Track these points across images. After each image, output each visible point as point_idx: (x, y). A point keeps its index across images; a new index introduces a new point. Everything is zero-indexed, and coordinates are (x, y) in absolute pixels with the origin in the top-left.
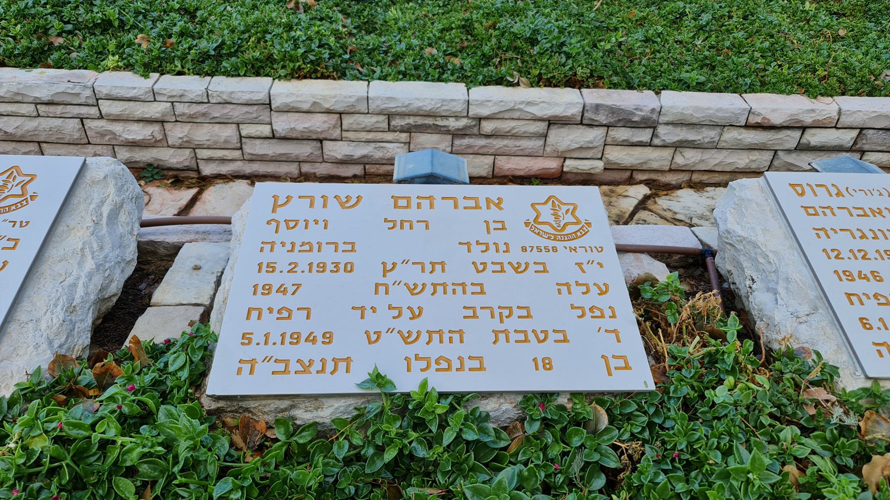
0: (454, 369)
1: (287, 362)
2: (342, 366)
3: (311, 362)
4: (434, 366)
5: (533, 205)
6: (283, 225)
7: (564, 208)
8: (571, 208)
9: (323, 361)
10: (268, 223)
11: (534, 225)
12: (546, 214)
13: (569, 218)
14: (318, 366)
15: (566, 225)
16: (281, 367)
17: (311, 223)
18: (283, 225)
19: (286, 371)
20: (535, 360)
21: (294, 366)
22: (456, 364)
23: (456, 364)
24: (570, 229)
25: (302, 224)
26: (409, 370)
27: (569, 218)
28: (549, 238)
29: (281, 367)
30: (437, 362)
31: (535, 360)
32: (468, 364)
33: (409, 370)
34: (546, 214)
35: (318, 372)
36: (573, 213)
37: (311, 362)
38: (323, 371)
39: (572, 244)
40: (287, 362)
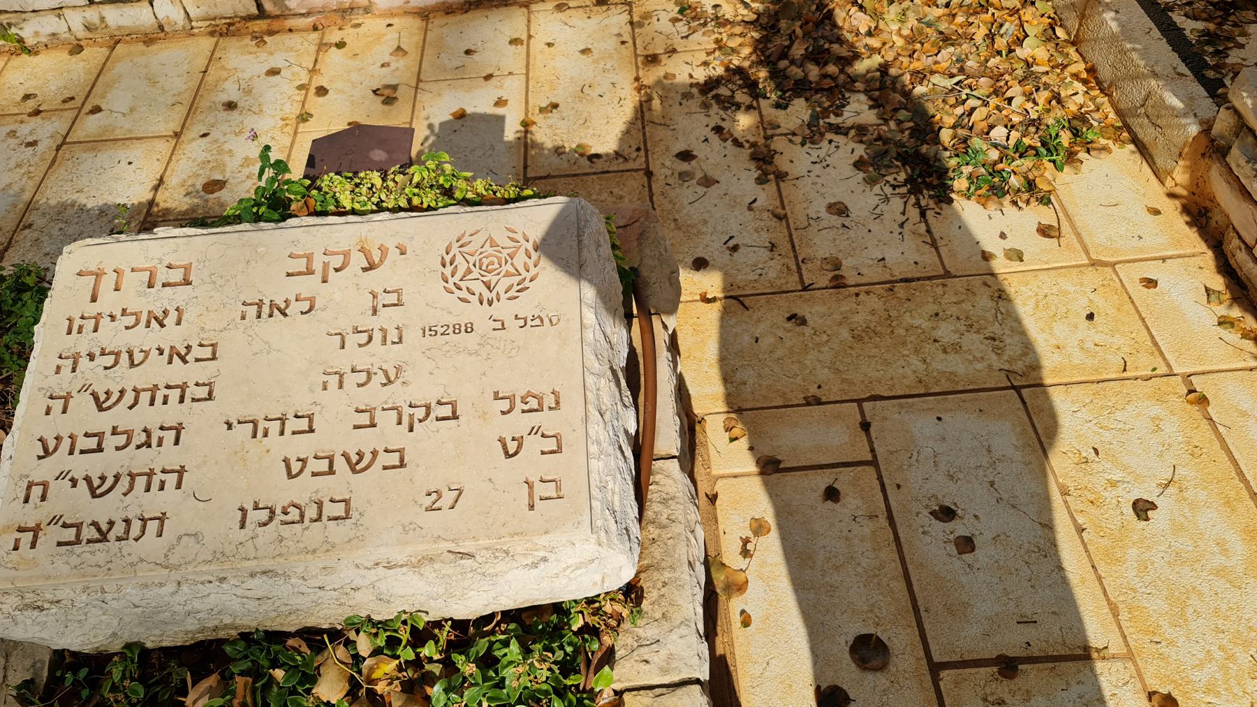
0: (306, 520)
1: (78, 526)
2: (153, 526)
3: (111, 523)
4: (280, 517)
9: (127, 521)
14: (119, 529)
16: (70, 534)
19: (78, 541)
21: (89, 533)
22: (311, 512)
23: (311, 512)
29: (70, 534)
35: (119, 539)
37: (111, 523)
40: (78, 526)
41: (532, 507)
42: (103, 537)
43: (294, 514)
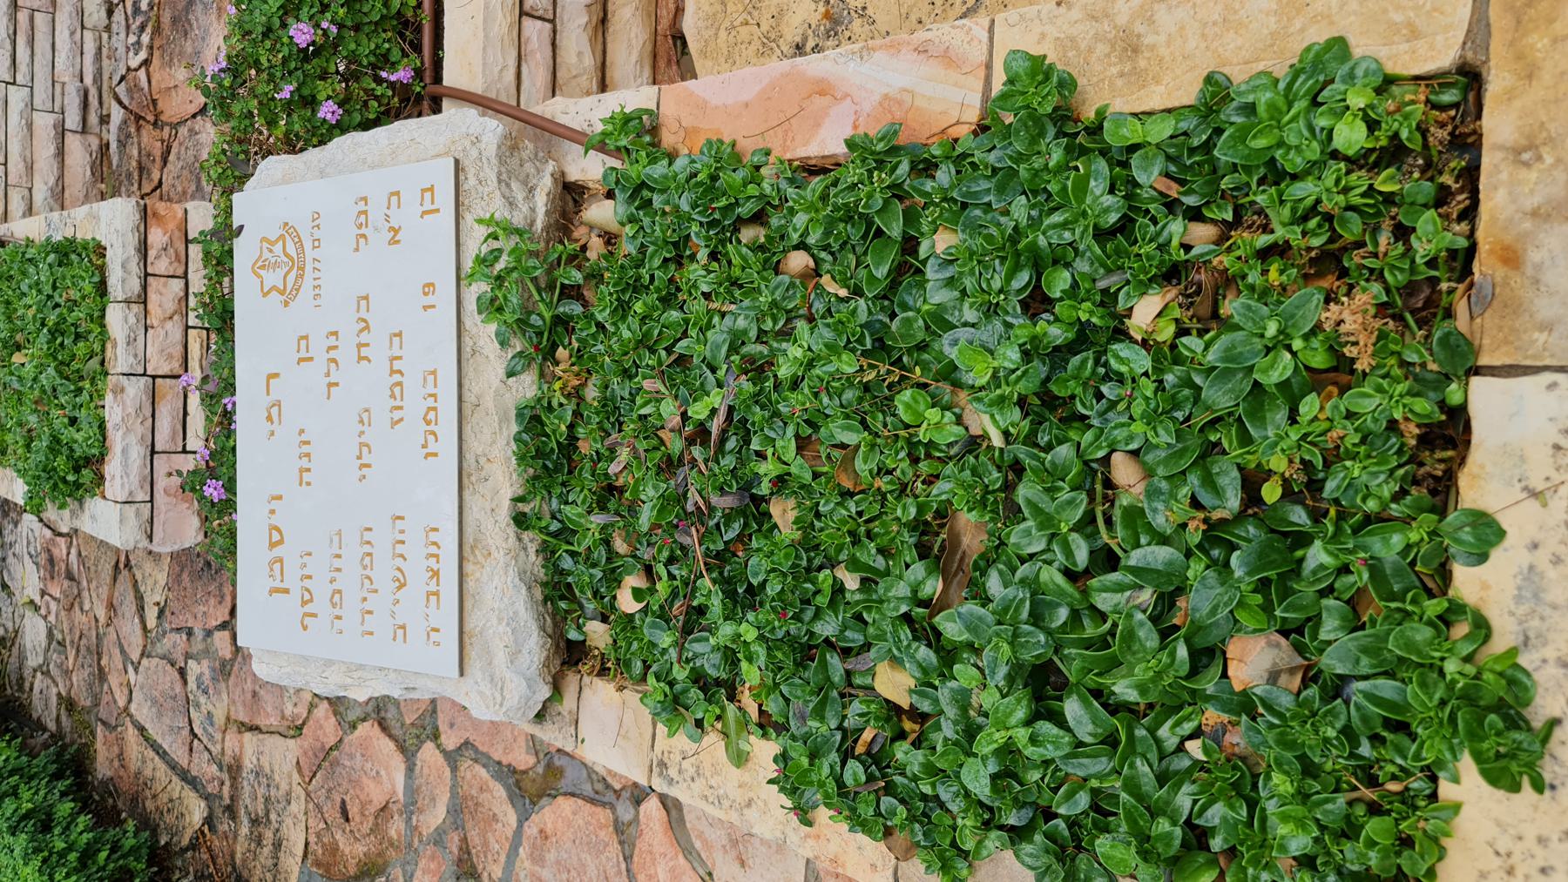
1: (429, 594)
4: (432, 427)
5: (265, 295)
6: (309, 608)
7: (267, 254)
8: (265, 245)
10: (305, 628)
11: (287, 295)
12: (272, 278)
13: (278, 248)
15: (286, 255)
17: (306, 572)
18: (309, 608)
19: (437, 594)
20: (425, 308)
24: (291, 250)
25: (307, 583)
26: (436, 455)
27: (278, 248)
28: (302, 276)
29: (433, 599)
30: (428, 423)
31: (425, 308)
32: (430, 389)
33: (436, 455)
34: (272, 278)
36: (273, 243)
38: (437, 556)
39: (308, 245)
40: (429, 594)
41: (438, 210)
42: (436, 574)
43: (431, 415)
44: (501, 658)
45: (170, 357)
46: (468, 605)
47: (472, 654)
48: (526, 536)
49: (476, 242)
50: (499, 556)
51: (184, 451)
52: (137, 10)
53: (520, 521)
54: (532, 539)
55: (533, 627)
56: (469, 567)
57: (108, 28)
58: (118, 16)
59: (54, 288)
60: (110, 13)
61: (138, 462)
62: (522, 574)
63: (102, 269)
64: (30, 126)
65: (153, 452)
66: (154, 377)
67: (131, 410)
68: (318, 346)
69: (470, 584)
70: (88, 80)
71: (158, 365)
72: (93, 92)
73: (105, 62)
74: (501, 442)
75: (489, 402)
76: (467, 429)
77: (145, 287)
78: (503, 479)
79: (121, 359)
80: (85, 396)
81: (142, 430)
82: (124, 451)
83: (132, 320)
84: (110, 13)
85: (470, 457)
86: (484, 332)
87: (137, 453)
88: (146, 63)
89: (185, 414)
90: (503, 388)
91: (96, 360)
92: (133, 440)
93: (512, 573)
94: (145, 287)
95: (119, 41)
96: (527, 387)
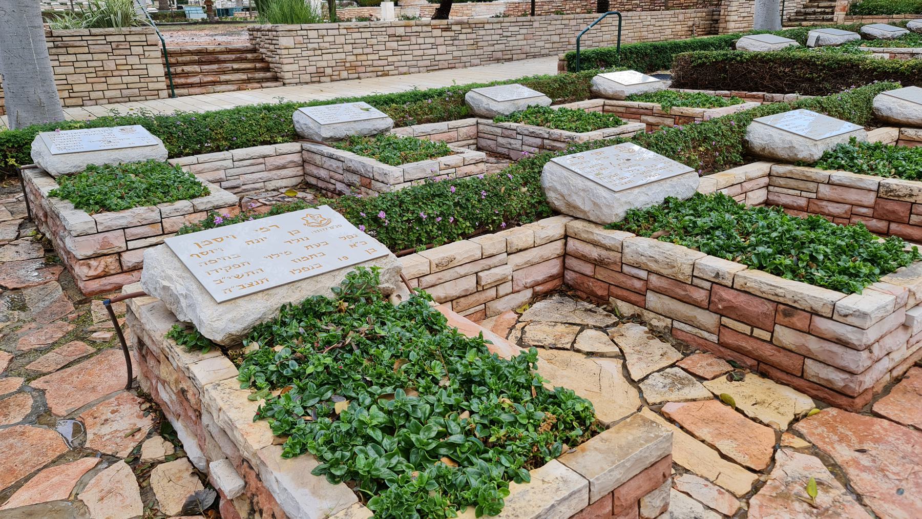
27: (320, 219)
42: (252, 285)
44: (230, 316)
45: (172, 226)
46: (246, 298)
47: (228, 305)
48: (277, 312)
49: (367, 267)
50: (269, 304)
51: (127, 241)
52: (283, 198)
53: (284, 307)
54: (277, 314)
55: (245, 325)
56: (260, 295)
57: (267, 191)
58: (275, 193)
59: (180, 182)
60: (274, 190)
61: (118, 224)
62: (265, 314)
63: (200, 196)
64: (218, 169)
65: (124, 229)
66: (161, 222)
67: (144, 216)
68: (297, 236)
69: (254, 297)
70: (244, 187)
71: (167, 224)
72: (240, 190)
73: (253, 192)
74: (309, 293)
75: (319, 285)
76: (308, 281)
77: (201, 211)
78: (296, 297)
79: (166, 208)
80: (137, 200)
81: (135, 222)
82: (123, 217)
83: (186, 209)
84: (274, 190)
85: (299, 284)
86: (342, 277)
87: (124, 222)
88: (265, 205)
89: (146, 238)
90: (326, 288)
91: (158, 201)
92: (130, 219)
93: (263, 310)
94: (201, 211)
95: (264, 195)
96: (331, 296)
